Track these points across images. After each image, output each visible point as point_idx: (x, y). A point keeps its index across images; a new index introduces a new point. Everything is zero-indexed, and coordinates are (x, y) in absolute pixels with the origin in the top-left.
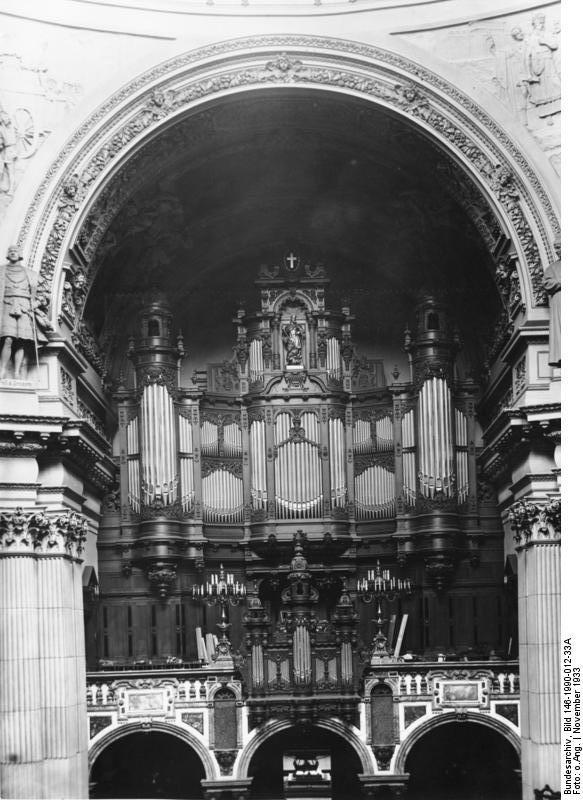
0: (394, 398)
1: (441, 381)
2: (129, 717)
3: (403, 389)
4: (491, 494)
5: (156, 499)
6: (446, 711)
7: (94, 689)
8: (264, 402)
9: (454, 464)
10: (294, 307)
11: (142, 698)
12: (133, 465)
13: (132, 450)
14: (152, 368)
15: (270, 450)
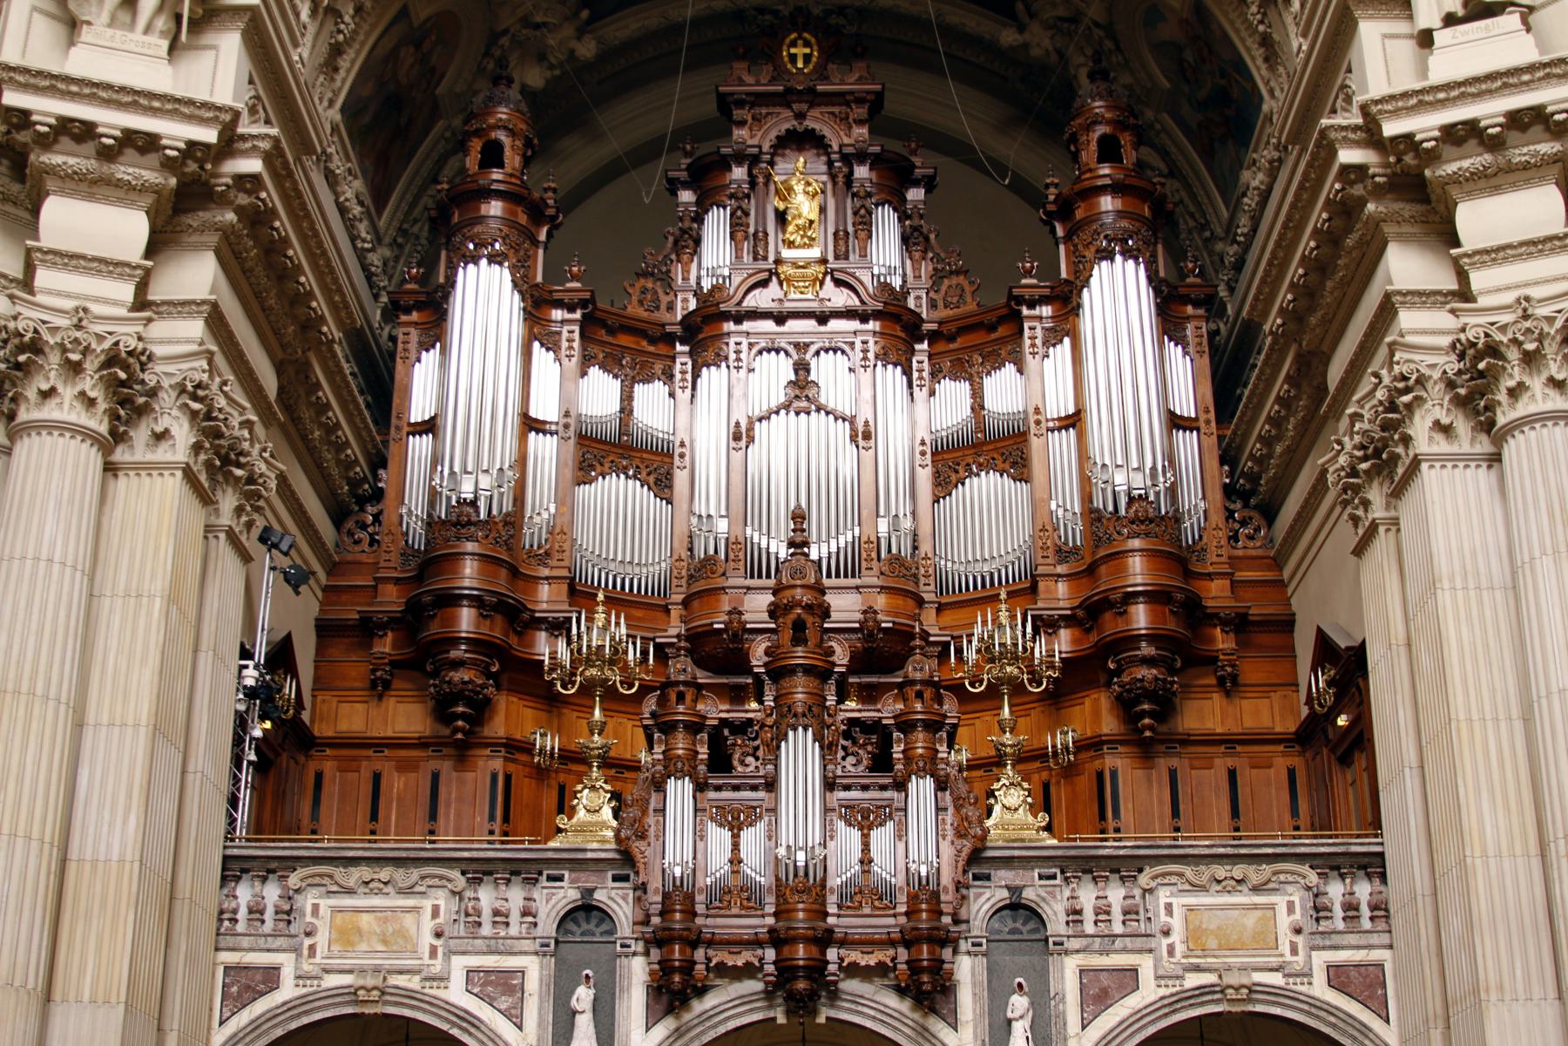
0: (1025, 311)
1: (1131, 263)
2: (327, 971)
3: (1047, 292)
4: (1257, 530)
5: (462, 503)
6: (1193, 980)
7: (244, 893)
8: (730, 326)
9: (1171, 458)
10: (800, 149)
11: (365, 917)
12: (420, 447)
13: (419, 410)
14: (478, 229)
15: (738, 424)
